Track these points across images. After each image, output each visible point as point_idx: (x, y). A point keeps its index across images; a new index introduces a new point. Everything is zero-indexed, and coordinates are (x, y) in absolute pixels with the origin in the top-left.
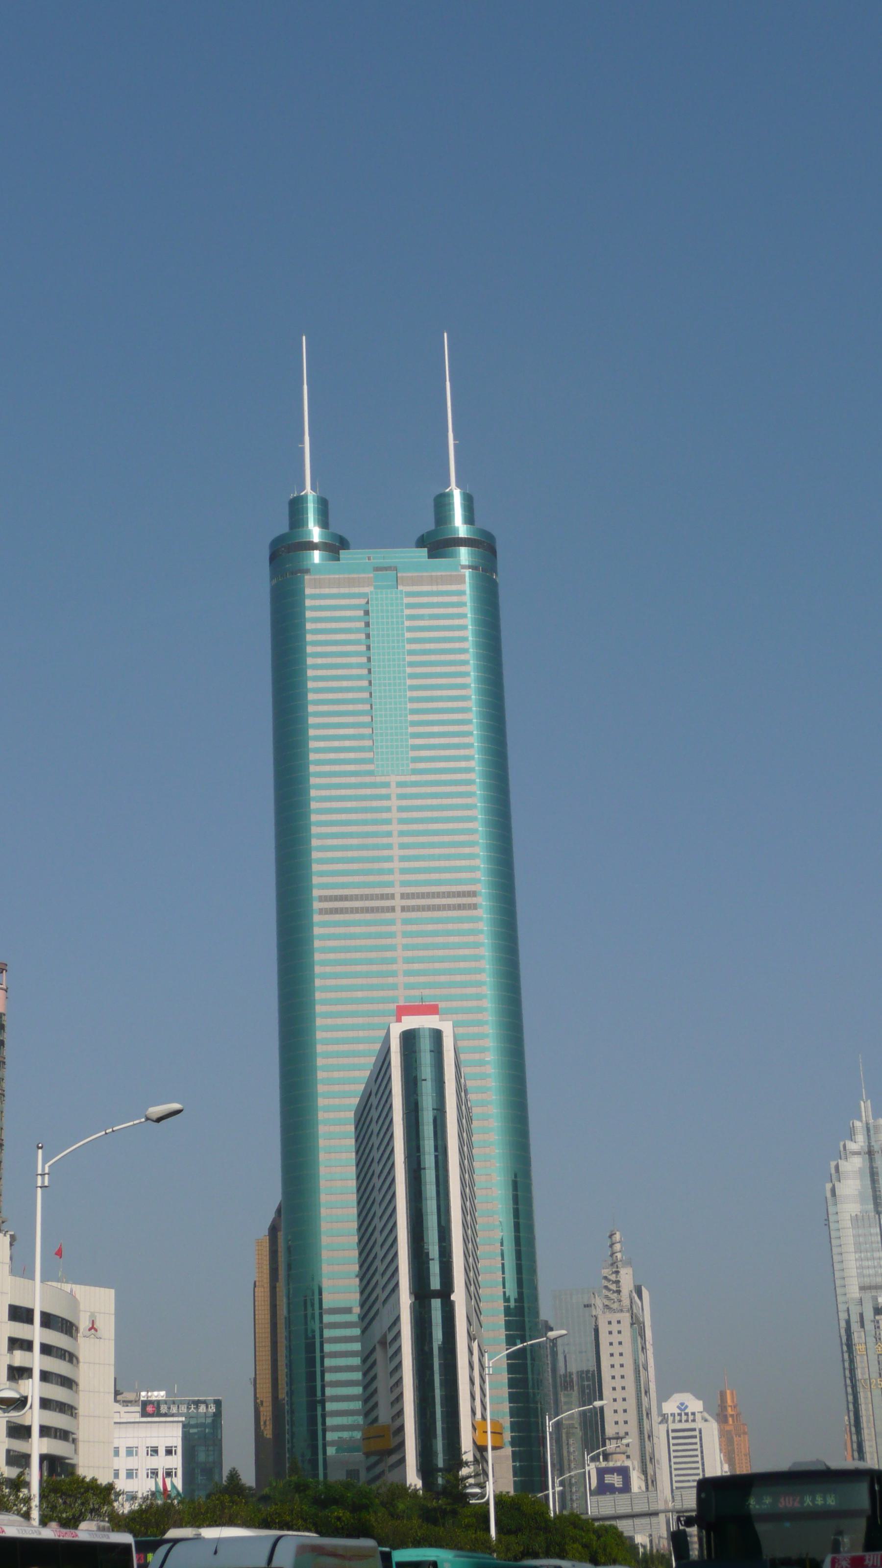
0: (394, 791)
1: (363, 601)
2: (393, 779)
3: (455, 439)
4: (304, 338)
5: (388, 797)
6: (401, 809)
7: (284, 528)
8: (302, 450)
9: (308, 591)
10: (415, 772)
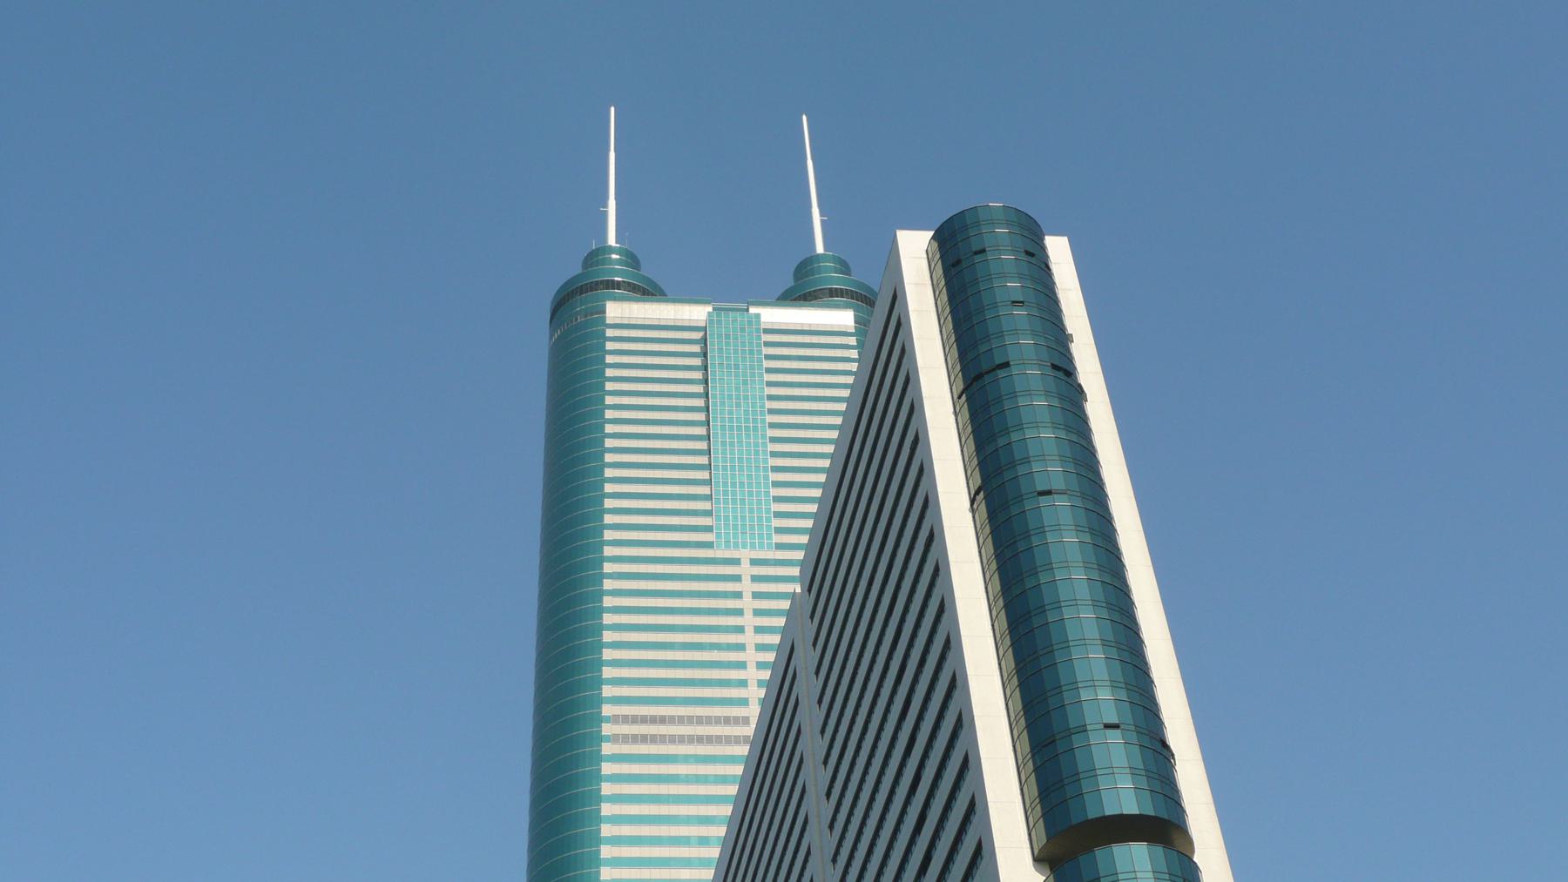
0: (746, 570)
1: (696, 348)
2: (745, 554)
3: (822, 214)
4: (613, 109)
5: (737, 578)
6: (756, 595)
7: (572, 268)
8: (606, 213)
9: (607, 322)
10: (780, 546)
